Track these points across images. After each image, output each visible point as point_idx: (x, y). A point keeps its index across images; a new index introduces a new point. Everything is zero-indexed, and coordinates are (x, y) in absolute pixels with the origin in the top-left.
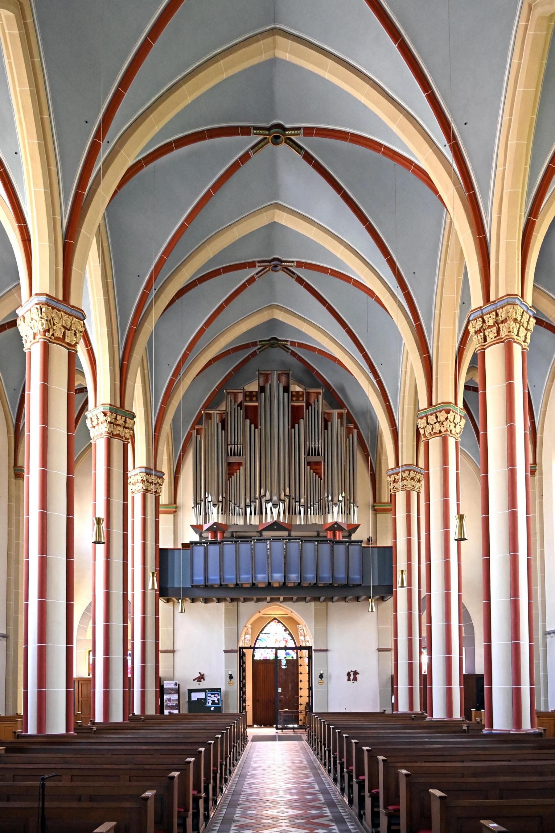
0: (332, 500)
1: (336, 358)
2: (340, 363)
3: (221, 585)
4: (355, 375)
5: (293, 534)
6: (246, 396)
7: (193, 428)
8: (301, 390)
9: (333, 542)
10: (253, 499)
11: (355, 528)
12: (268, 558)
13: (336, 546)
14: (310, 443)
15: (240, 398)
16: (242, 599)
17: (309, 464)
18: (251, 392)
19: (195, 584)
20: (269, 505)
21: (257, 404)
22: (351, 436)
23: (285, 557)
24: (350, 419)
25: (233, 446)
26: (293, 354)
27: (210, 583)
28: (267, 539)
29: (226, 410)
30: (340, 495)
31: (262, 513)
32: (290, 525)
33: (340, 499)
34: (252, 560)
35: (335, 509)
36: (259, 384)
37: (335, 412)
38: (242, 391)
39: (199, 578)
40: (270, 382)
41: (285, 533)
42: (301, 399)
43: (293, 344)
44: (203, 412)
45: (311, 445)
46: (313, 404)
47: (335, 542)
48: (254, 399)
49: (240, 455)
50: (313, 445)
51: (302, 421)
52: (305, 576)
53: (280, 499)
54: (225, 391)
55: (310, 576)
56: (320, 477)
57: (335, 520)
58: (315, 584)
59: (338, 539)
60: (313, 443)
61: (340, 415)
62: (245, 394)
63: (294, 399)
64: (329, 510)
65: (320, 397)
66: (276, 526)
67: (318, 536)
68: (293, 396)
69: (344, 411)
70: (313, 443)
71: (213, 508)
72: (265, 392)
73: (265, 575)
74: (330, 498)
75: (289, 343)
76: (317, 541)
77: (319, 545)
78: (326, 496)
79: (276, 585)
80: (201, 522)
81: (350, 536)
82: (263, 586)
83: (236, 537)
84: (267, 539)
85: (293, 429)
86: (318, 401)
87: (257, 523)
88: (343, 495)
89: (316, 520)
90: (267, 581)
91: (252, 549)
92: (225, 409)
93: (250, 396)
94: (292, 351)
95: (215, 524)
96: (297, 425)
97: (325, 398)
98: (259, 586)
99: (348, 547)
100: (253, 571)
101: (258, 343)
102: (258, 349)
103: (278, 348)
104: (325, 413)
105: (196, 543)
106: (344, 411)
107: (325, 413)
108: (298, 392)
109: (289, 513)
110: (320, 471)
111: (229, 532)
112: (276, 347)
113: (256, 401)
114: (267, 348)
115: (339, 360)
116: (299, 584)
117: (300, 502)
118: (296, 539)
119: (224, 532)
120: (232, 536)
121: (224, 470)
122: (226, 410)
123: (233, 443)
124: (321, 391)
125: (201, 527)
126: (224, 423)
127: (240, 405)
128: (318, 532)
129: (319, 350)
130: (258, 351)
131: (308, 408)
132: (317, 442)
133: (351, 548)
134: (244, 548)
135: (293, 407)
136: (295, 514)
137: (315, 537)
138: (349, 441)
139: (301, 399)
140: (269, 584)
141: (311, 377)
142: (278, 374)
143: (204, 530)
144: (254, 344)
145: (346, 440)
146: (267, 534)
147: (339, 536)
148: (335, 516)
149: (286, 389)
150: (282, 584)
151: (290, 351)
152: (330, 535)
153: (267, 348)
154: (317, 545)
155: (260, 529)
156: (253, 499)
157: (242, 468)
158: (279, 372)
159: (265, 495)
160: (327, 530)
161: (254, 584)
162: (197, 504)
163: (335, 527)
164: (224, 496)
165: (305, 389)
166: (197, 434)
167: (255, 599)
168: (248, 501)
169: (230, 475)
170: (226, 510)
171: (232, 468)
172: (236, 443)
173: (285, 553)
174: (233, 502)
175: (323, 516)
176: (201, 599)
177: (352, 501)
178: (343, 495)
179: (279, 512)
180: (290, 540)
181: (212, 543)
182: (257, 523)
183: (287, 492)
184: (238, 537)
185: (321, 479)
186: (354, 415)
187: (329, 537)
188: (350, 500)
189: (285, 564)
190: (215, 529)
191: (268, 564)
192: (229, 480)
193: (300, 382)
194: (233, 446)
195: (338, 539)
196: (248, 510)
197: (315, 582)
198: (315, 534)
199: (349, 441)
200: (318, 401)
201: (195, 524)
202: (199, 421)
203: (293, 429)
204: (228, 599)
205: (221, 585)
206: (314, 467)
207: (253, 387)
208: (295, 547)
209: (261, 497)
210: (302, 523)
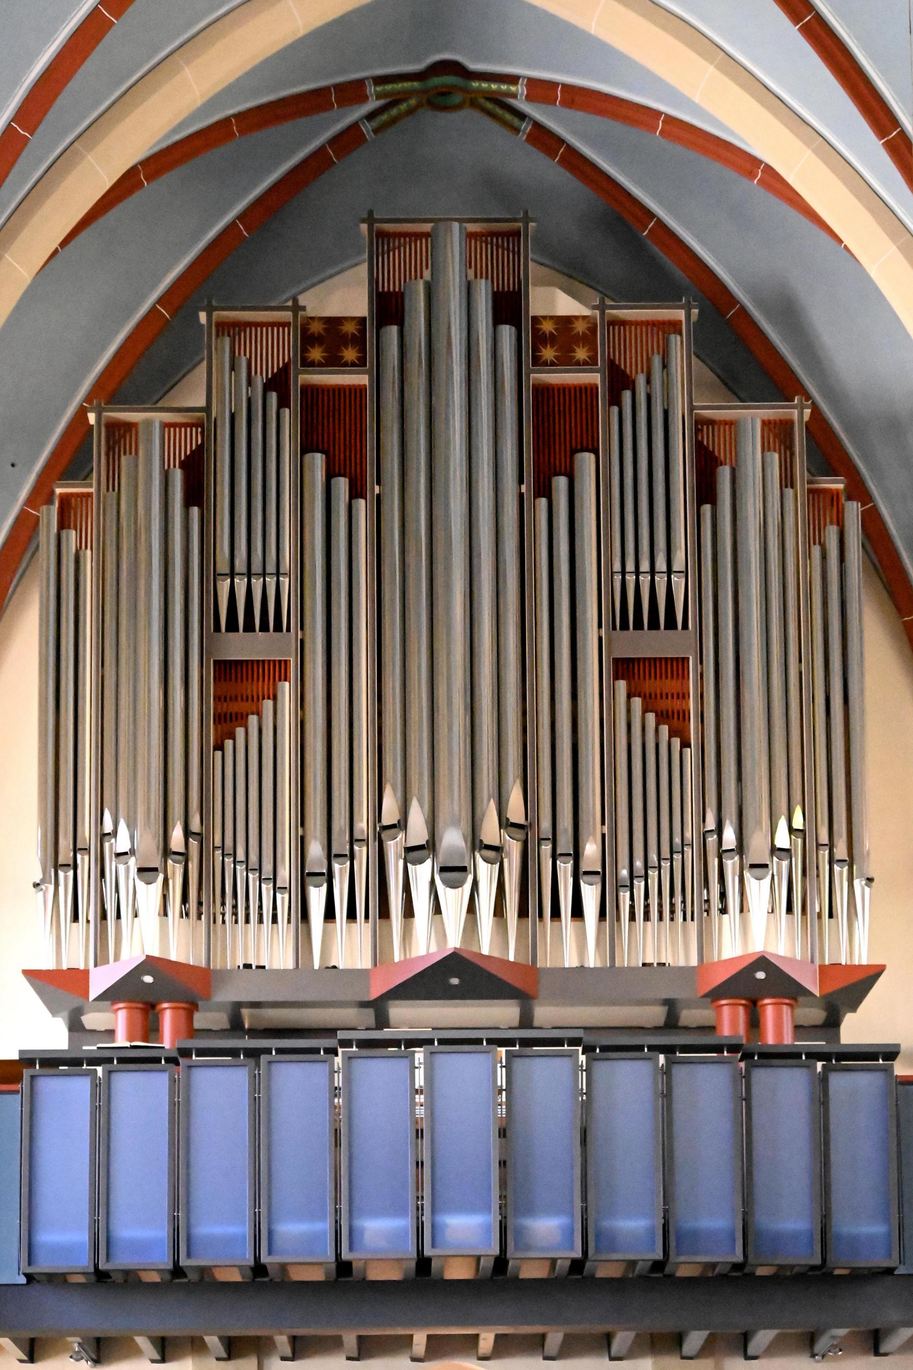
0: (741, 848)
1: (755, 162)
2: (774, 183)
3: (177, 1271)
4: (847, 241)
5: (546, 1014)
6: (308, 339)
7: (41, 494)
8: (586, 312)
9: (747, 1056)
11: (855, 985)
12: (419, 1134)
13: (762, 1077)
14: (630, 567)
15: (277, 350)
16: (282, 1341)
17: (624, 668)
18: (333, 323)
19: (44, 1266)
20: (422, 873)
21: (362, 379)
22: (832, 533)
23: (503, 1133)
24: (827, 452)
25: (241, 585)
26: (544, 139)
27: (122, 1261)
28: (413, 1043)
29: (207, 409)
30: (782, 825)
31: (384, 912)
32: (530, 970)
33: (782, 840)
34: (337, 1143)
35: (758, 890)
36: (373, 282)
37: (753, 418)
38: (287, 316)
39: (65, 1237)
40: (427, 274)
41: (502, 1014)
42: (581, 354)
43: (542, 90)
44: (92, 418)
45: (631, 579)
46: (641, 380)
47: (756, 1056)
48: (350, 354)
49: (278, 628)
50: (645, 580)
51: (586, 460)
52: (606, 1224)
53: (476, 844)
54: (203, 317)
55: (633, 1228)
56: (679, 732)
57: (757, 946)
58: (658, 1266)
59: (770, 1040)
60: (645, 566)
61: (779, 434)
62: (304, 330)
63: (548, 353)
64: (723, 895)
65: (678, 346)
66: (456, 976)
67: (671, 1023)
68: (540, 339)
69: (797, 414)
70: (645, 566)
71: (140, 885)
72: (401, 323)
73: (404, 1223)
74: (730, 836)
75: (520, 89)
76: (668, 1050)
77: (679, 1072)
78: (711, 824)
79: (458, 1271)
80: (76, 952)
81: (832, 1023)
82: (395, 1275)
83: (254, 1033)
84: (413, 1043)
85: (543, 502)
86: (665, 366)
87: (364, 962)
88: (798, 823)
89: (661, 944)
90: (412, 1252)
91: (335, 1092)
92: (202, 403)
93: (330, 339)
94: (538, 126)
95: (150, 964)
96: (561, 483)
97: (703, 345)
98: (375, 1274)
99: (824, 1080)
100: (343, 1197)
101: (371, 89)
102: (371, 116)
103: (468, 114)
104: (700, 425)
105: (51, 1062)
106: (797, 414)
107: (700, 425)
108: (566, 322)
109: (523, 913)
110: (677, 704)
111: (219, 1007)
112: (459, 107)
113: (361, 362)
114: (411, 112)
115: (769, 169)
116: (577, 1266)
117: (577, 855)
118: (558, 1042)
119: (191, 1007)
120: (236, 1026)
121: (194, 699)
122: (207, 409)
124: (680, 314)
125: (75, 980)
126: (196, 469)
127: (278, 383)
128: (670, 1004)
129: (671, 120)
130: (367, 128)
131: (615, 400)
132: (661, 565)
133: (839, 1082)
134: (297, 1084)
135: (543, 392)
136: (556, 913)
137: (657, 1029)
138: (824, 557)
139: (581, 354)
140: (423, 1264)
141: (631, 247)
142: (471, 236)
143: (94, 993)
144: (351, 92)
145: (809, 555)
146: (408, 1017)
147: (778, 1025)
148: (757, 928)
149: (508, 307)
150: (487, 1264)
151: (526, 127)
152: (730, 1021)
153: (411, 112)
154: (667, 1072)
155: (374, 994)
156: (341, 844)
157: (286, 690)
158: (472, 227)
159: (402, 825)
160: (716, 995)
161: (344, 1268)
162: (57, 866)
163: (759, 982)
164: (195, 826)
165: (602, 308)
166: (63, 524)
167: (350, 1340)
168: (316, 850)
170: (204, 894)
171: (235, 692)
172: (257, 567)
173: (502, 1111)
174: (241, 856)
175: (693, 927)
176: (74, 1342)
177: (841, 851)
178: (798, 823)
179: (472, 909)
180: (526, 1043)
181: (131, 1060)
183: (516, 813)
184: (265, 1034)
185: (685, 744)
186: (848, 429)
187: (726, 1031)
188: (831, 846)
189: (503, 1164)
190: (151, 990)
191: (419, 1164)
192: (220, 747)
193: (575, 273)
194: (241, 585)
195: (770, 1040)
196: (317, 897)
197: (658, 1255)
198: (656, 1015)
199: (824, 557)
200: (665, 366)
201: (48, 964)
202: (72, 458)
203: (543, 502)
204: (213, 1341)
205: (177, 1271)
206: (650, 685)
207: (345, 297)
208: (551, 1081)
209: (382, 832)
210: (592, 961)
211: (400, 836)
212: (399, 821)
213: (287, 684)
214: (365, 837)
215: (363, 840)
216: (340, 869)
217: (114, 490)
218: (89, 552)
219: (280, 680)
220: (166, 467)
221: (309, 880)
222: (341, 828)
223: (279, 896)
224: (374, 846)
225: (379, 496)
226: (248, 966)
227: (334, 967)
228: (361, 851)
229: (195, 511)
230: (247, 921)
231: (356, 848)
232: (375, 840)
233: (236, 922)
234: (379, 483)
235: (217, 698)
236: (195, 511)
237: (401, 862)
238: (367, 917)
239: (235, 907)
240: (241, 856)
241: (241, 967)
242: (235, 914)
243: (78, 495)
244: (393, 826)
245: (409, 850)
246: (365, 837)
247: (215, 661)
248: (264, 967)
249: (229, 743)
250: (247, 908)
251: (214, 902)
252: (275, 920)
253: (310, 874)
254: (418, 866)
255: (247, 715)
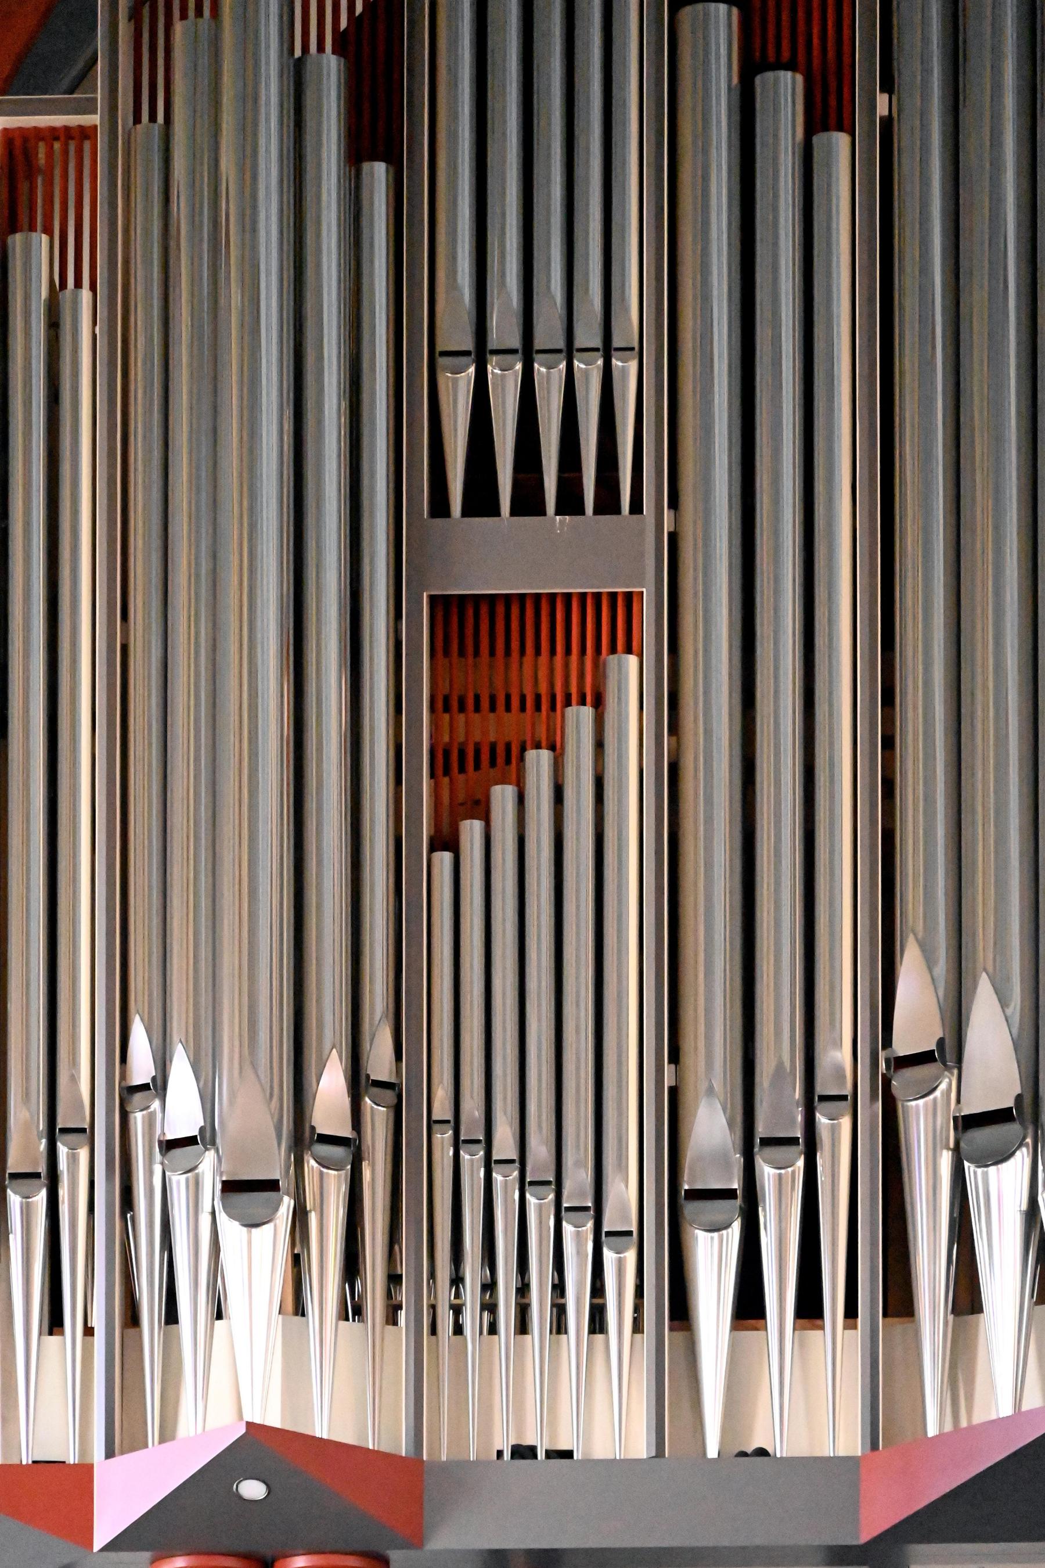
10: (779, 1110)
31: (899, 1300)
71: (231, 1230)
121: (374, 707)
123: (504, 329)
156: (779, 1110)
157: (630, 676)
159: (949, 1052)
164: (380, 1062)
168: (711, 1127)
169: (466, 770)
172: (548, 330)
174: (505, 1145)
182: (847, 1440)
192: (446, 840)
194: (505, 383)
209: (894, 1073)
211: (943, 1086)
212: (941, 1043)
213: (632, 660)
214: (848, 1090)
215: (844, 1098)
216: (778, 1181)
217: (153, 118)
218: (86, 294)
219: (613, 650)
220: (298, 53)
221: (690, 1209)
222: (780, 1066)
223: (609, 1256)
224: (871, 1112)
225: (887, 123)
226: (523, 1452)
227: (762, 1452)
228: (834, 1131)
229: (378, 172)
230: (523, 1327)
231: (822, 1120)
232: (873, 1097)
233: (493, 1330)
234: (888, 86)
235: (441, 704)
236: (378, 172)
237: (946, 1160)
238: (851, 1312)
239: (489, 1286)
240: (505, 1145)
241: (507, 1455)
242: (490, 1307)
243: (53, 134)
244: (924, 1058)
245: (968, 1123)
246: (848, 1090)
247: (432, 599)
248: (568, 1454)
249: (471, 830)
250: (523, 1290)
251: (432, 1275)
252: (597, 1322)
253: (696, 1195)
254: (992, 1170)
255: (523, 749)
